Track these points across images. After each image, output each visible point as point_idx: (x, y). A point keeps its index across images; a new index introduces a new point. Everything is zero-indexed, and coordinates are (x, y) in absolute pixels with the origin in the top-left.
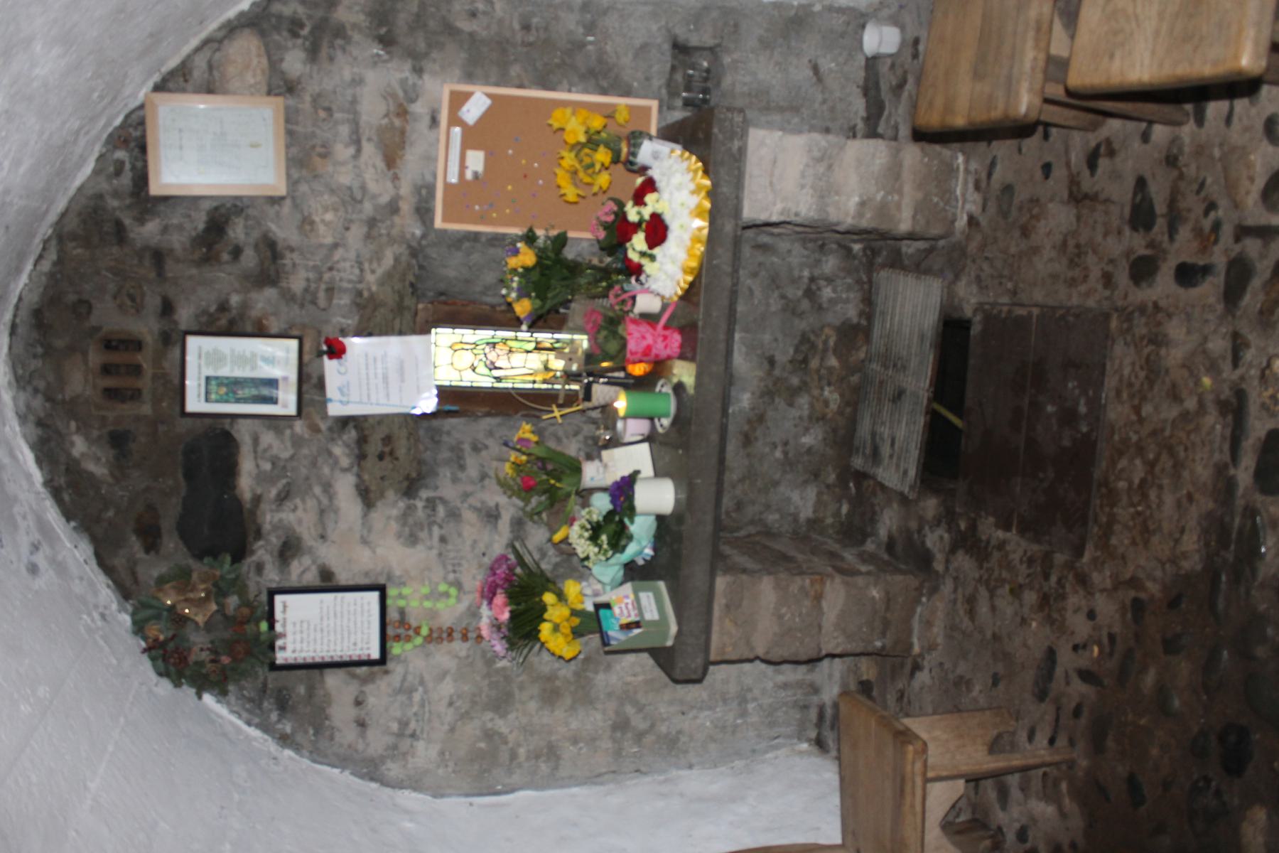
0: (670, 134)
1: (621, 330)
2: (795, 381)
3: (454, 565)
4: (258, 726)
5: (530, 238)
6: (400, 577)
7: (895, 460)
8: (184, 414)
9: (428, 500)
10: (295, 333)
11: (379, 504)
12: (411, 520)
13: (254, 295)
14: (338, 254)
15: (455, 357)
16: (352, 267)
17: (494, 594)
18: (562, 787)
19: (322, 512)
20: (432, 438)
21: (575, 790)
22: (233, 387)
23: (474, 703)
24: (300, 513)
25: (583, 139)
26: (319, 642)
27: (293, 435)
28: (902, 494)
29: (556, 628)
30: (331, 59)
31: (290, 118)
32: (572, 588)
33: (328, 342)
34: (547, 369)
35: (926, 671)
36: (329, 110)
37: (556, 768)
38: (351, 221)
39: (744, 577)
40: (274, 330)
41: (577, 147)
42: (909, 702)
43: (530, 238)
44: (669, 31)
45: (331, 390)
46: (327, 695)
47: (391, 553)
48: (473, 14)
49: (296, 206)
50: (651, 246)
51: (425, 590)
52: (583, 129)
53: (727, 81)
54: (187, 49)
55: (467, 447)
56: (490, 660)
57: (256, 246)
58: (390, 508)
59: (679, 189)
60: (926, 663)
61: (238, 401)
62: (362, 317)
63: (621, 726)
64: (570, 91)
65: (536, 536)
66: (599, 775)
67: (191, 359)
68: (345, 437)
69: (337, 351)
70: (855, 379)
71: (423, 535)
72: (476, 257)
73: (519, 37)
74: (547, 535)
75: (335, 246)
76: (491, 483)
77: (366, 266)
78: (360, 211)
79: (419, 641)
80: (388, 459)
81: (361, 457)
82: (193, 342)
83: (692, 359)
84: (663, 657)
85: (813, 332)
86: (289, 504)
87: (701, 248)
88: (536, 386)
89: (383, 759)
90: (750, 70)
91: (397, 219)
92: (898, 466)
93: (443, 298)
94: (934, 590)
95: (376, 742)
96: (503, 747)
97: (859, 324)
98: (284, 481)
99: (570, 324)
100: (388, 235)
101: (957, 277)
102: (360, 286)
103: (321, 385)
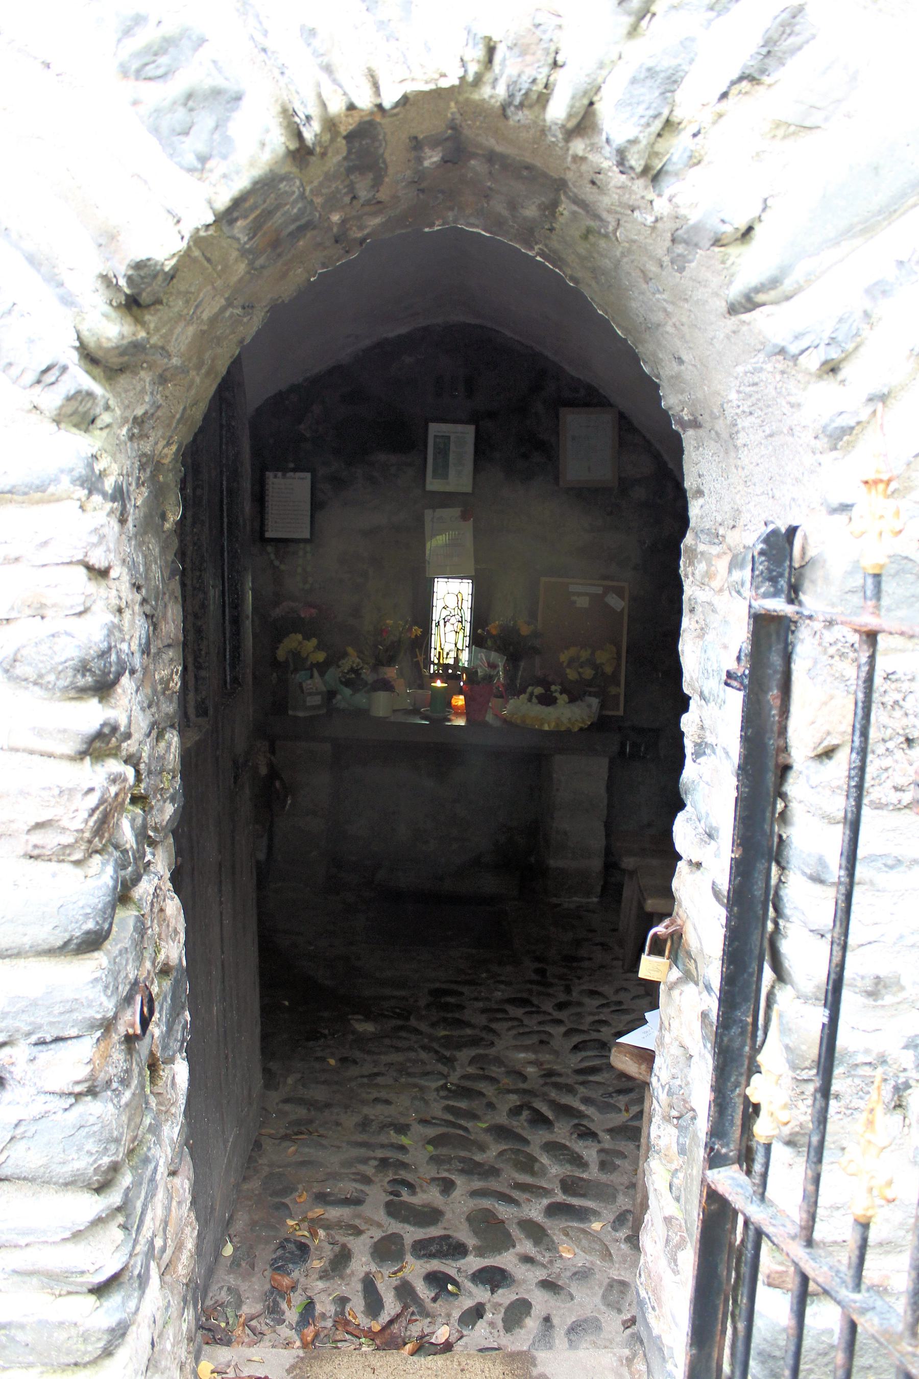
22: (443, 452)
45: (440, 512)
67: (460, 427)
69: (464, 517)
82: (470, 429)
103: (443, 506)
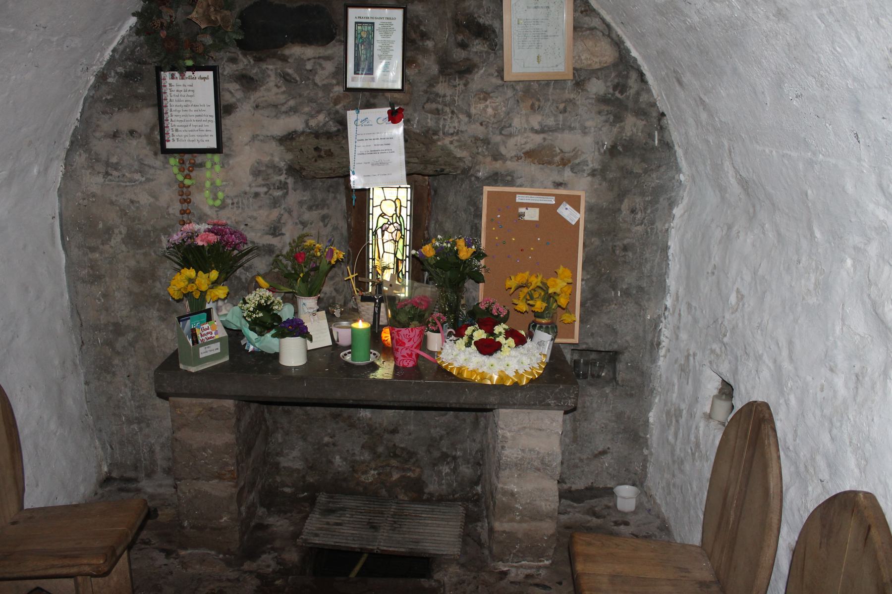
0: (556, 351)
1: (415, 323)
2: (380, 449)
3: (238, 203)
4: (112, 56)
5: (478, 255)
6: (229, 164)
7: (325, 526)
8: (347, 6)
9: (286, 183)
10: (406, 88)
11: (282, 148)
12: (270, 171)
13: (433, 57)
14: (464, 119)
15: (390, 200)
16: (455, 127)
17: (216, 234)
18: (69, 286)
19: (276, 106)
20: (331, 186)
21: (67, 296)
22: (366, 41)
23: (133, 220)
24: (275, 90)
25: (551, 291)
26: (179, 104)
27: (332, 85)
28: (301, 533)
29: (191, 281)
30: (600, 113)
31: (558, 83)
32: (221, 291)
33: (401, 110)
34: (384, 268)
35: (166, 561)
36: (565, 111)
37: (84, 282)
38: (487, 127)
39: (234, 420)
40: (408, 72)
41: (544, 287)
42: (141, 550)
43: (478, 255)
44: (626, 348)
45: (365, 113)
46: (138, 110)
47: (245, 157)
48: (633, 211)
49: (497, 87)
50: (476, 343)
51: (218, 182)
52: (558, 291)
53: (593, 391)
54: (603, 13)
55: (325, 211)
56: (166, 231)
57: (468, 59)
58: (279, 156)
59: (517, 362)
60: (172, 560)
61: (356, 46)
62: (419, 134)
63: (118, 330)
64: (582, 280)
65: (261, 264)
66: (79, 314)
68: (331, 123)
70: (384, 492)
71: (260, 180)
72: (463, 215)
73: (619, 244)
74: (262, 272)
75: (469, 116)
76: (299, 231)
77: (456, 138)
78: (494, 134)
79: (180, 178)
80: (315, 154)
81: (317, 135)
82: (398, 14)
83: (395, 375)
84: (172, 362)
85: (417, 460)
86: (281, 82)
87: (477, 379)
89: (88, 151)
90: (601, 406)
91: (489, 159)
92: (321, 529)
93: (433, 193)
94: (228, 563)
95: (102, 146)
96: (99, 242)
97: (424, 493)
98: (298, 79)
99: (416, 284)
100: (478, 153)
101: (463, 566)
102: (441, 133)
103: (369, 106)
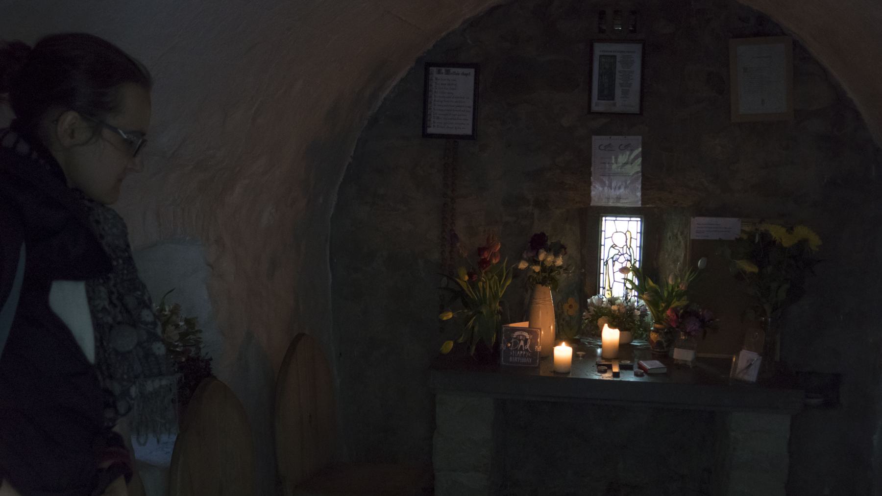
61: (600, 75)
88: (601, 289)
